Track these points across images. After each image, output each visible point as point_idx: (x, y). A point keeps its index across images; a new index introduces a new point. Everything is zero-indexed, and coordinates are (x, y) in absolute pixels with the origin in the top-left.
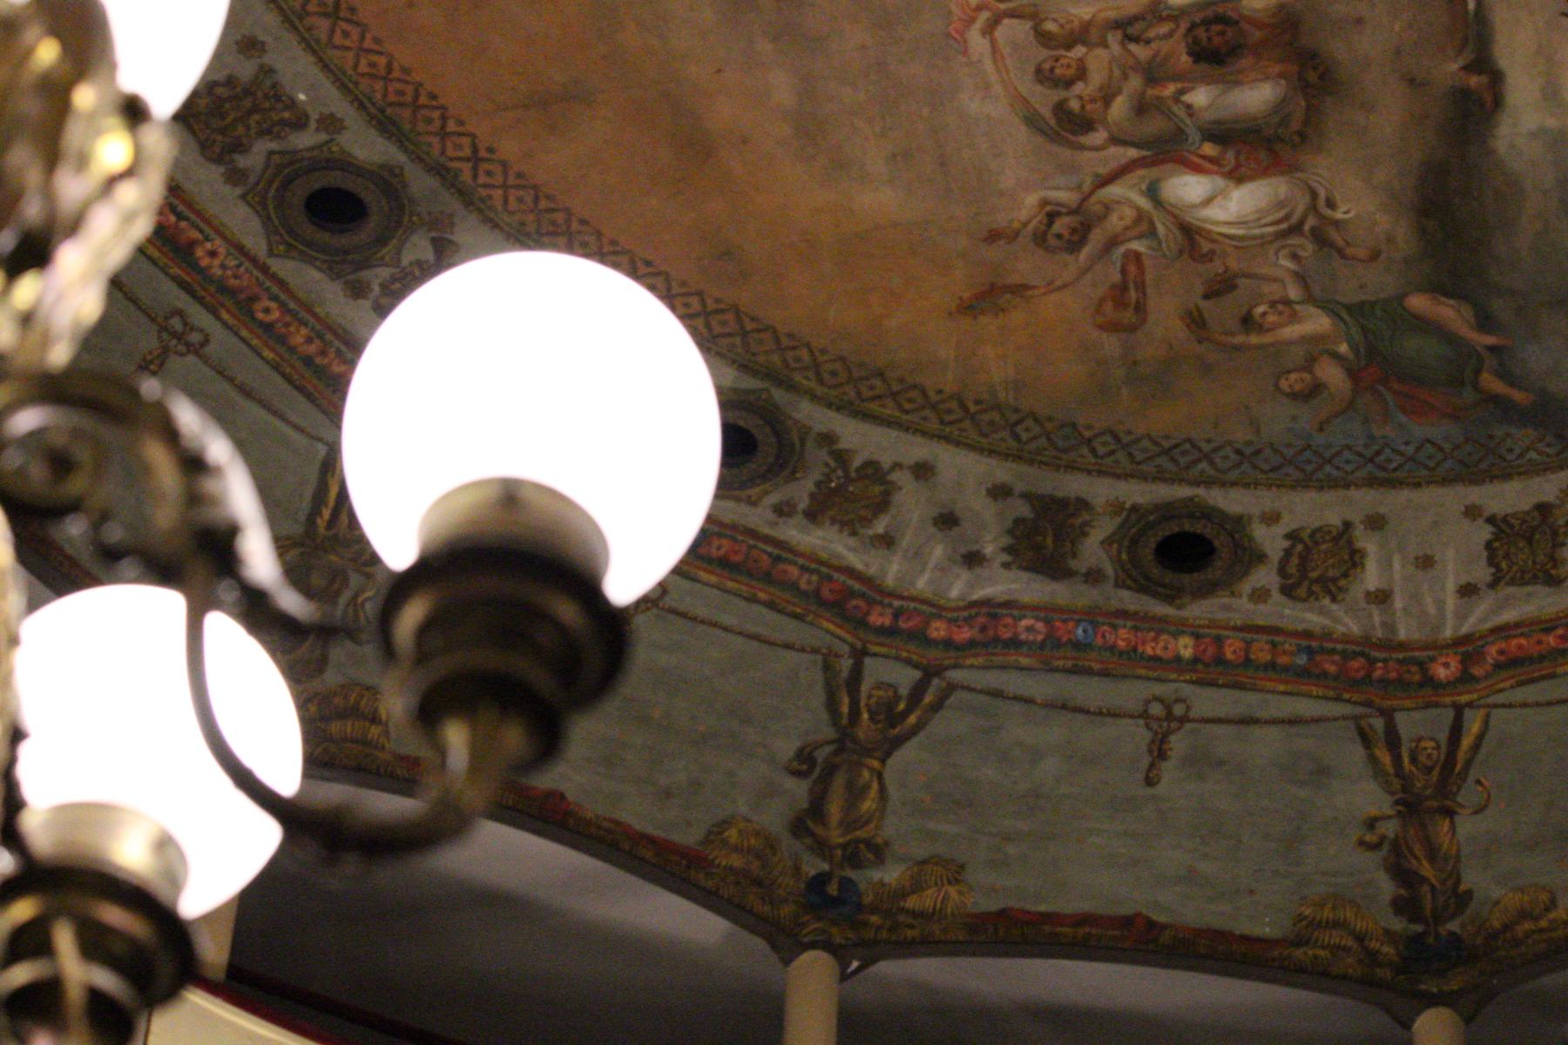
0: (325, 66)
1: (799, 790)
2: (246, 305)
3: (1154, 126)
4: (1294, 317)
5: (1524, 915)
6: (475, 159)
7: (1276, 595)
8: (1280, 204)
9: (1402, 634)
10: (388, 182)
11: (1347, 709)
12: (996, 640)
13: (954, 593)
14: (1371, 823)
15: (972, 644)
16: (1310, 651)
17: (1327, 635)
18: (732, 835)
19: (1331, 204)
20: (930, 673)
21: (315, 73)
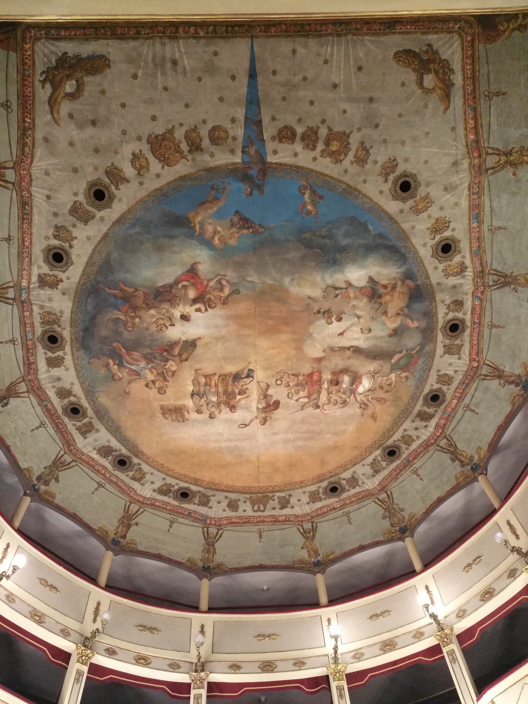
1: (457, 462)
3: (348, 392)
4: (391, 378)
8: (368, 378)
10: (330, 483)
12: (443, 427)
13: (432, 430)
14: (500, 384)
15: (443, 430)
16: (463, 383)
18: (458, 476)
20: (445, 437)
21: (311, 487)
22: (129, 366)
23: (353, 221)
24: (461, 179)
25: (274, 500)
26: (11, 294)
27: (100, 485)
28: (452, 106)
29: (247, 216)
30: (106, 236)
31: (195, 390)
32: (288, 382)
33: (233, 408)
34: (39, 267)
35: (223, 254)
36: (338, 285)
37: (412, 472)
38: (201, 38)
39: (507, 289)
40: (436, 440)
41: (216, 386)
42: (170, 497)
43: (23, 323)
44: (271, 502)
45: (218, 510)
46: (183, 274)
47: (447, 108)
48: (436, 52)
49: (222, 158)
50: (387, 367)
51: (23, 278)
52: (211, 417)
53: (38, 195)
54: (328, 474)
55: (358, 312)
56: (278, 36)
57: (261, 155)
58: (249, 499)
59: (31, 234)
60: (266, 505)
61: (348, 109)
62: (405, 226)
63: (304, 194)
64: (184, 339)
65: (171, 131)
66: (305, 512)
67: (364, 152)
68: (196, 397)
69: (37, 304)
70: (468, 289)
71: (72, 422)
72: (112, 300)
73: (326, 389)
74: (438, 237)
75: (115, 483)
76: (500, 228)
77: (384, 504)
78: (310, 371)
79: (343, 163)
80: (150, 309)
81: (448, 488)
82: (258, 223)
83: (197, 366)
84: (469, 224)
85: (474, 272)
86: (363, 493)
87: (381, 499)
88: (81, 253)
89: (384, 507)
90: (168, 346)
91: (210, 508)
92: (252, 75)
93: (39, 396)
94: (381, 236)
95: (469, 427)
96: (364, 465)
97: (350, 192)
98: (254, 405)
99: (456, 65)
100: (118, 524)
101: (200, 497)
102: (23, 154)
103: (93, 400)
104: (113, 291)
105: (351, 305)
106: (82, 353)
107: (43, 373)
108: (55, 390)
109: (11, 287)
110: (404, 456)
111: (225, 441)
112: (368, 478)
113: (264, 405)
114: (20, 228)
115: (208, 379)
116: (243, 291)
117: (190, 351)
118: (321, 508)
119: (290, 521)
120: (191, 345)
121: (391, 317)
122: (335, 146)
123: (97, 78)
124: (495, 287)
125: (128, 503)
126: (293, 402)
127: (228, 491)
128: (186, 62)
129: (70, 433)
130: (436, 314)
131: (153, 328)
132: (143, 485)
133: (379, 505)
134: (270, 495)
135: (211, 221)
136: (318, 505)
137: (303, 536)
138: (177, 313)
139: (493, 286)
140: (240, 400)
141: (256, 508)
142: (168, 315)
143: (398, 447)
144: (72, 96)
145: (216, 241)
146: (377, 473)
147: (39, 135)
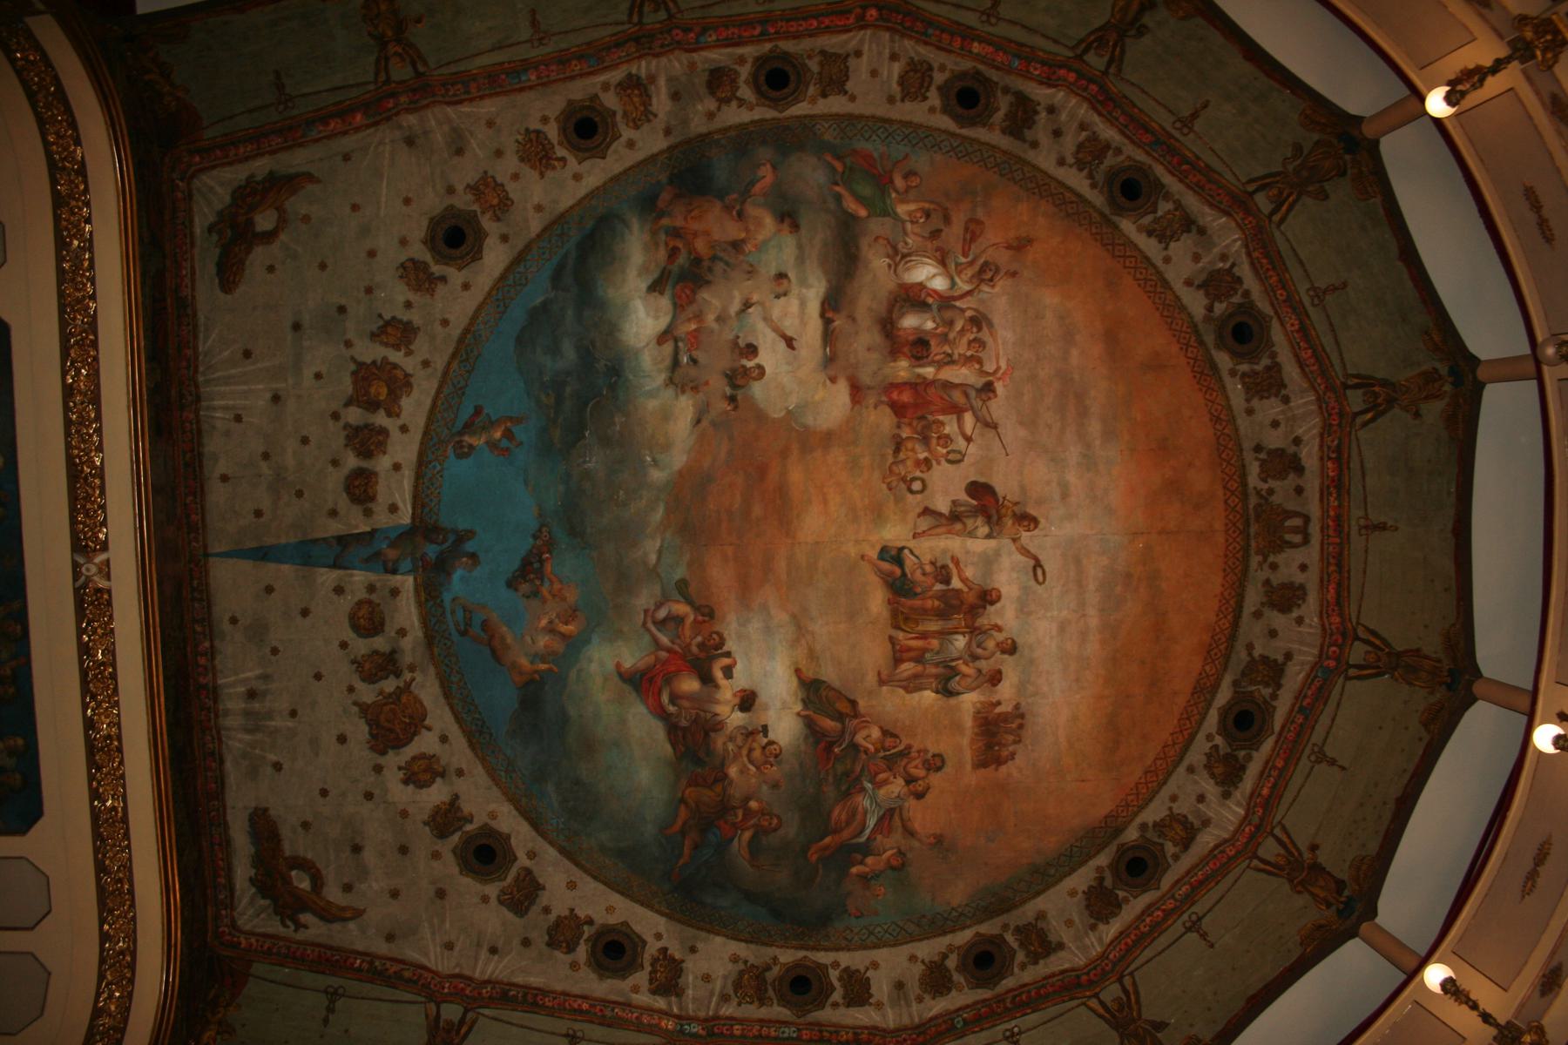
0: (1227, 398)
3: (948, 314)
4: (910, 213)
7: (936, 66)
8: (908, 269)
9: (887, 35)
10: (1221, 344)
15: (1060, 67)
17: (918, 41)
18: (1181, 13)
20: (1079, 57)
21: (1231, 396)
22: (868, 832)
23: (523, 341)
25: (1271, 491)
29: (516, 564)
30: (563, 851)
32: (918, 463)
33: (988, 597)
34: (636, 989)
36: (668, 362)
37: (1185, 130)
38: (212, 646)
41: (924, 636)
42: (1249, 758)
44: (1276, 499)
45: (1298, 638)
47: (310, 178)
48: (220, 213)
49: (406, 612)
50: (878, 226)
52: (1011, 648)
55: (735, 306)
56: (203, 508)
58: (1265, 560)
59: (564, 994)
60: (1286, 512)
61: (315, 369)
62: (535, 225)
63: (471, 447)
64: (799, 707)
65: (364, 709)
66: (1313, 407)
67: (390, 330)
68: (954, 684)
69: (718, 1005)
71: (1016, 970)
73: (939, 368)
74: (561, 152)
76: (534, 23)
78: (888, 410)
79: (409, 370)
80: (726, 776)
82: (531, 540)
83: (871, 678)
84: (531, 88)
85: (639, 58)
86: (1255, 254)
88: (602, 905)
91: (1288, 656)
92: (263, 554)
94: (557, 277)
96: (1167, 260)
97: (466, 349)
98: (979, 545)
99: (236, 174)
100: (1306, 896)
101: (1252, 682)
104: (686, 850)
105: (715, 326)
107: (884, 1016)
108: (927, 997)
110: (1140, 156)
113: (980, 521)
114: (551, 1012)
115: (906, 655)
116: (680, 573)
117: (831, 694)
118: (1301, 365)
119: (1339, 446)
120: (813, 691)
121: (747, 230)
122: (380, 391)
123: (285, 832)
125: (1255, 862)
126: (972, 449)
128: (249, 674)
131: (773, 772)
132: (1206, 823)
134: (1253, 501)
136: (1291, 371)
137: (1383, 413)
138: (737, 719)
139: (668, 10)
140: (964, 580)
141: (1297, 539)
143: (1112, 175)
144: (317, 880)
146: (1194, 222)
147: (382, 948)
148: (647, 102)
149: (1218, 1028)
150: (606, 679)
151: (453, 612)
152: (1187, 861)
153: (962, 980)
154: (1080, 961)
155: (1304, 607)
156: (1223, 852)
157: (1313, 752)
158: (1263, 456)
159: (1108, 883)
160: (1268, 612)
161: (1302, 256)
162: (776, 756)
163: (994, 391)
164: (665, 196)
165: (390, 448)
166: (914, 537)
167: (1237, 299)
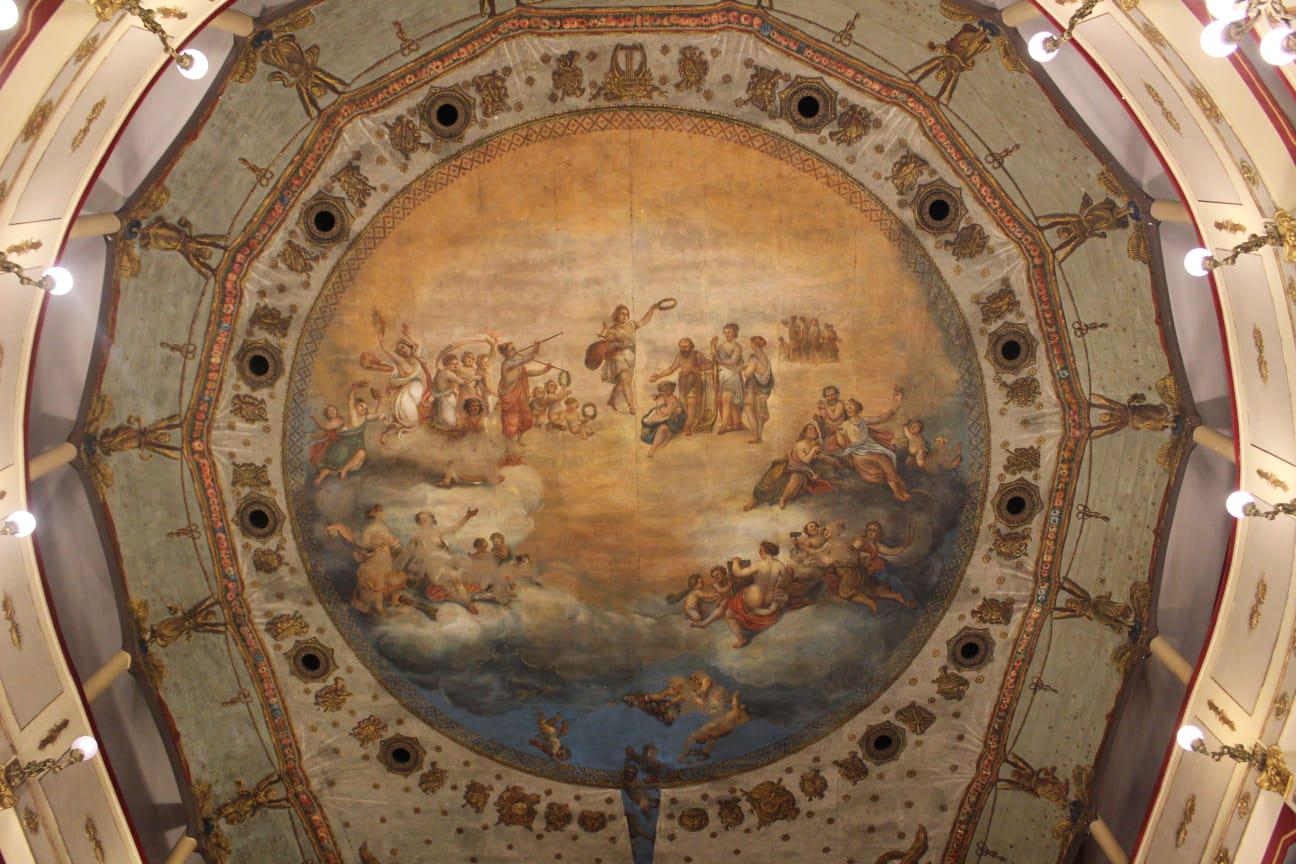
0: (509, 129)
1: (174, 220)
2: (415, 72)
3: (442, 384)
4: (360, 415)
5: (103, 476)
6: (460, 168)
8: (406, 417)
9: (215, 433)
10: (457, 136)
11: (183, 413)
12: (225, 296)
13: (247, 285)
14: (138, 420)
15: (224, 288)
16: (209, 402)
17: (216, 407)
18: (164, 196)
19: (404, 432)
20: (214, 272)
22: (888, 452)
23: (478, 711)
24: (316, 763)
25: (593, 84)
26: (1063, 598)
27: (998, 159)
28: (357, 852)
29: (653, 719)
30: (884, 688)
31: (762, 396)
32: (570, 410)
33: (687, 350)
34: (1004, 635)
35: (695, 662)
36: (490, 607)
37: (268, 175)
39: (187, 606)
40: (234, 260)
41: (719, 405)
42: (844, 101)
43: (1059, 541)
46: (767, 627)
47: (363, 848)
50: (372, 440)
51: (1036, 621)
52: (733, 329)
53: (975, 740)
54: (466, 163)
57: (631, 798)
58: (655, 88)
60: (612, 70)
61: (505, 849)
62: (390, 700)
63: (561, 748)
64: (777, 508)
65: (763, 823)
66: (513, 42)
68: (763, 380)
70: (253, 593)
71: (1023, 321)
72: (895, 580)
74: (330, 681)
75: (963, 158)
76: (233, 702)
77: (320, 79)
78: (525, 435)
79: (504, 788)
80: (832, 565)
81: (181, 165)
82: (635, 709)
83: (755, 449)
84: (283, 702)
87: (329, 91)
88: (933, 657)
89: (318, 73)
90: (807, 493)
91: (748, 63)
93: (1072, 391)
95: (171, 309)
96: (385, 188)
97: (488, 749)
100: (977, 58)
102: (980, 794)
103: (971, 374)
106: (970, 476)
107: (1051, 436)
109: (1059, 609)
110: (295, 213)
111: (705, 262)
112: (369, 147)
113: (619, 357)
115: (736, 421)
116: (661, 601)
118: (474, 57)
119: (549, 19)
120: (764, 496)
121: (382, 545)
124: (208, 603)
125: (943, 99)
126: (557, 363)
127: (703, 114)
129: (1033, 296)
130: (300, 549)
131: (830, 528)
132: (902, 144)
133: (332, 77)
134: (602, 102)
135: (713, 711)
136: (481, 67)
138: (784, 558)
139: (212, 605)
141: (637, 56)
142: (800, 555)
143: (313, 239)
145: (705, 682)
146: (350, 163)
147: (950, 815)
148: (288, 618)
149: (1092, 155)
150: (747, 656)
151: (690, 762)
152: (936, 161)
153: (1027, 369)
154: (1020, 263)
155: (702, 49)
156: (931, 128)
157: (841, 42)
158: (560, 93)
159: (951, 237)
160: (706, 86)
161: (375, 61)
162: (817, 526)
163: (507, 345)
164: (359, 606)
165: (564, 802)
166: (633, 414)
167: (416, 121)
